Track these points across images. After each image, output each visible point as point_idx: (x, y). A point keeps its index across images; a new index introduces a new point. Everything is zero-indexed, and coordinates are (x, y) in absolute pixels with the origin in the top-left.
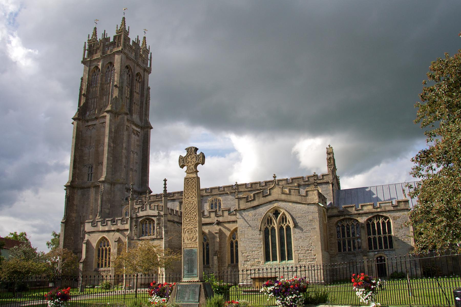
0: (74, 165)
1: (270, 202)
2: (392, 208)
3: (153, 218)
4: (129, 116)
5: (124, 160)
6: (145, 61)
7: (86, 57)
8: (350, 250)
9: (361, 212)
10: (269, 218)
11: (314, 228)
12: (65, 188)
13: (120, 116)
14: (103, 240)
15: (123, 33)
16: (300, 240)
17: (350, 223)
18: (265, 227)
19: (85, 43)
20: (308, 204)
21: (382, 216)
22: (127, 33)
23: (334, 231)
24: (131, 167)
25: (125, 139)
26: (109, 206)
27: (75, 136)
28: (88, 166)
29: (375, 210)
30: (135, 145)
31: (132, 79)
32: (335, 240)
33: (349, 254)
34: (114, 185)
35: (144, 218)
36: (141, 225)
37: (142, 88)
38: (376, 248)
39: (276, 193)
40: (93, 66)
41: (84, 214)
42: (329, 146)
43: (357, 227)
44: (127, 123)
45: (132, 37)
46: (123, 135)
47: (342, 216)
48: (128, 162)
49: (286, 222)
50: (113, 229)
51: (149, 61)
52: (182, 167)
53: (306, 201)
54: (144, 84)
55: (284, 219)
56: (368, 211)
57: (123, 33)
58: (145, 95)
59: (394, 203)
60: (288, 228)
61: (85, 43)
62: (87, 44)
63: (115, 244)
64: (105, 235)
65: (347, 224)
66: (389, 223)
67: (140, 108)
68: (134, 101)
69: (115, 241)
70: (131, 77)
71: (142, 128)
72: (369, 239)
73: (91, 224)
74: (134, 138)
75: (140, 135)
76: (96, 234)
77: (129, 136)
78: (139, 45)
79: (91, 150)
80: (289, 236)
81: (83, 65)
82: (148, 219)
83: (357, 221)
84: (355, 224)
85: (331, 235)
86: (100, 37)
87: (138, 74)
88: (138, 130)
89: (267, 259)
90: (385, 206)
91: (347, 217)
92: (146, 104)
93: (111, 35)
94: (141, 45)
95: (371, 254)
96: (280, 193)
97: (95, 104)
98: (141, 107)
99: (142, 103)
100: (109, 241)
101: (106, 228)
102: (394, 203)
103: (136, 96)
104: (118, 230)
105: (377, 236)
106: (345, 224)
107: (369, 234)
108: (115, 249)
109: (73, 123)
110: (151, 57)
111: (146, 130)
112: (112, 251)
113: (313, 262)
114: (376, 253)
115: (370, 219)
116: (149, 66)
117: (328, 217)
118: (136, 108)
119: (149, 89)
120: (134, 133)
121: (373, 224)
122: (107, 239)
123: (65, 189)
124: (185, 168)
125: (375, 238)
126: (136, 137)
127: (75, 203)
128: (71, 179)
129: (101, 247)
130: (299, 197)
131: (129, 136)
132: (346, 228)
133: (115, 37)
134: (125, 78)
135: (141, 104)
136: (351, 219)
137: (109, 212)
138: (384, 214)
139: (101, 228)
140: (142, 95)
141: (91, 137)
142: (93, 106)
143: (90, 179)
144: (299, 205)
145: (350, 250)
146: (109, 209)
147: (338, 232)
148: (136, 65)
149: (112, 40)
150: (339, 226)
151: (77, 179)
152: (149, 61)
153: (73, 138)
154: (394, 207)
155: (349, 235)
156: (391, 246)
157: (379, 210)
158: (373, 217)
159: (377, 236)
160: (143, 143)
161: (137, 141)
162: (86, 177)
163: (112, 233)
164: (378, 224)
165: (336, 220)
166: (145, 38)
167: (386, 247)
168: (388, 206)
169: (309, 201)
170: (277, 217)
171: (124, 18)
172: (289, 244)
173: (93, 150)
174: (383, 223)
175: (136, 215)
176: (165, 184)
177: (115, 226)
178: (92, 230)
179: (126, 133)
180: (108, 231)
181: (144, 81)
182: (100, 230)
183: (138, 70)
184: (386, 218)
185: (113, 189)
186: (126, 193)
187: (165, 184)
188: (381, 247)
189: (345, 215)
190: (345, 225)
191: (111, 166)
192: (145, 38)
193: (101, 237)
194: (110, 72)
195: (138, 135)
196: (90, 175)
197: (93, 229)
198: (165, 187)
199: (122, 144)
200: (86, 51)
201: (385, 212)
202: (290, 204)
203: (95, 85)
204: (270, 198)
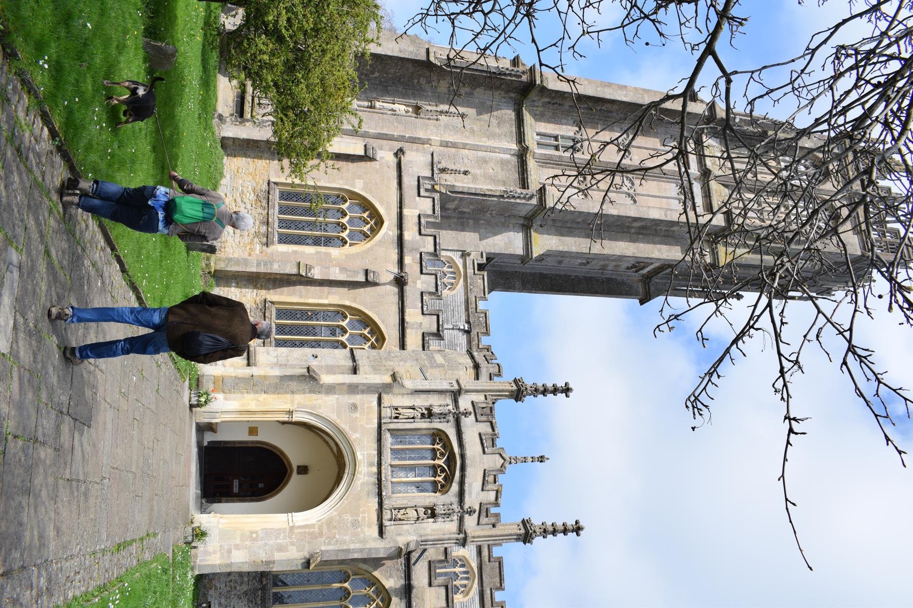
3: (455, 487)
28: (578, 136)
34: (523, 225)
35: (456, 450)
41: (443, 118)
50: (407, 260)
63: (356, 273)
64: (388, 229)
69: (367, 272)
73: (428, 174)
75: (631, 273)
82: (451, 460)
100: (369, 245)
101: (410, 234)
104: (400, 282)
108: (343, 269)
111: (640, 288)
112: (334, 252)
122: (375, 230)
127: (478, 90)
137: (449, 209)
139: (410, 214)
146: (455, 209)
151: (547, 100)
160: (609, 280)
163: (395, 257)
175: (466, 414)
178: (405, 179)
182: (406, 212)
185: (513, 221)
193: (382, 211)
195: (632, 267)
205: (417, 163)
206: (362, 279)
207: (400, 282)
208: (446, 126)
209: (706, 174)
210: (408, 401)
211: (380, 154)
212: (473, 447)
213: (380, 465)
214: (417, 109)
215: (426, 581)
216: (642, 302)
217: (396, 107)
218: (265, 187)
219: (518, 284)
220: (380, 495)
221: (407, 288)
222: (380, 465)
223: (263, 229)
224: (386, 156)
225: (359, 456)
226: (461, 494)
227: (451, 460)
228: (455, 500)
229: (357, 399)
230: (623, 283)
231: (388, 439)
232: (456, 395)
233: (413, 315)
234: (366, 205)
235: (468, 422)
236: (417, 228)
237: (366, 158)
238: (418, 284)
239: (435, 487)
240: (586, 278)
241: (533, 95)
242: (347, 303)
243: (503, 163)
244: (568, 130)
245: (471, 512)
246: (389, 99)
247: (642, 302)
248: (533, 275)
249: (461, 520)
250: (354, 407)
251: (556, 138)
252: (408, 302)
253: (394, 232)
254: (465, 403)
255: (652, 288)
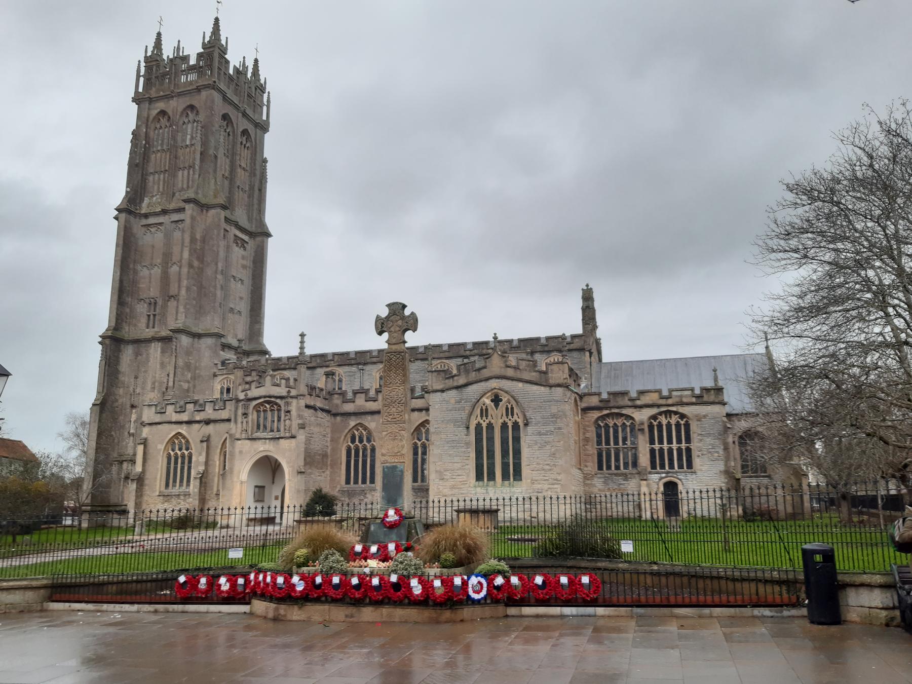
0: (120, 297)
1: (487, 379)
2: (694, 400)
3: (278, 401)
4: (228, 211)
5: (219, 293)
6: (257, 105)
7: (140, 90)
8: (617, 468)
9: (638, 403)
10: (484, 408)
11: (560, 428)
12: (100, 339)
13: (212, 212)
14: (178, 438)
15: (214, 49)
16: (536, 447)
17: (619, 422)
18: (476, 422)
19: (139, 62)
20: (551, 386)
21: (676, 413)
22: (223, 51)
23: (592, 434)
24: (232, 306)
25: (222, 254)
26: (189, 375)
27: (121, 243)
28: (147, 301)
29: (663, 402)
30: (240, 266)
31: (234, 142)
32: (592, 449)
33: (616, 475)
35: (262, 400)
36: (255, 413)
37: (251, 159)
38: (662, 466)
39: (496, 365)
40: (156, 109)
41: (138, 391)
42: (587, 285)
43: (631, 431)
44: (224, 225)
45: (234, 59)
46: (218, 246)
47: (606, 408)
48: (226, 297)
49: (512, 415)
50: (198, 418)
51: (265, 108)
52: (380, 333)
53: (547, 380)
54: (256, 151)
55: (509, 411)
56: (651, 402)
57: (214, 49)
58: (258, 173)
59: (697, 392)
60: (516, 426)
61: (139, 62)
62: (143, 64)
64: (183, 430)
65: (615, 424)
66: (687, 425)
67: (249, 197)
68: (238, 183)
69: (202, 441)
70: (231, 137)
71: (251, 234)
72: (652, 451)
73: (153, 408)
74: (237, 252)
75: (248, 247)
76: (166, 426)
77: (228, 247)
78: (246, 74)
79: (152, 272)
80: (517, 440)
81: (135, 107)
83: (632, 418)
84: (628, 424)
85: (587, 440)
86: (168, 52)
87: (245, 132)
88: (246, 238)
89: (479, 477)
90: (681, 396)
91: (616, 411)
92: (260, 190)
93: (193, 49)
94: (249, 75)
95: (655, 477)
96: (503, 365)
97: (161, 183)
98: (250, 196)
99: (252, 188)
100: (190, 440)
101: (184, 417)
102: (697, 392)
103: (242, 177)
104: (208, 422)
105: (665, 446)
106: (611, 422)
107: (652, 442)
108: (200, 454)
109: (116, 218)
110: (268, 101)
111: (259, 239)
112: (194, 459)
113: (556, 486)
114: (664, 475)
115: (654, 417)
116: (264, 118)
117: (582, 410)
118: (241, 197)
119: (265, 161)
120: (237, 243)
121: (660, 426)
122: (184, 437)
123: (100, 343)
124: (386, 336)
125: (661, 450)
126: (241, 252)
128: (113, 324)
129: (173, 450)
130: (534, 374)
131: (228, 247)
132: (611, 430)
133: (200, 55)
134: (222, 140)
135: (250, 189)
136: (622, 415)
137: (189, 388)
138: (681, 410)
139: (175, 417)
140: (253, 174)
141: (153, 247)
142: (156, 187)
143: (151, 325)
144: (535, 387)
145: (617, 468)
146: (189, 382)
147: (599, 436)
148: (240, 115)
149: (193, 62)
150: (599, 425)
152: (265, 108)
153: (117, 245)
154: (698, 397)
155: (616, 443)
156: (690, 465)
157: (670, 401)
158: (660, 414)
159: (665, 446)
160: (254, 262)
161: (243, 258)
162: (144, 321)
164: (669, 425)
165: (596, 414)
166: (256, 61)
167: (681, 466)
168: (686, 396)
169: (552, 382)
170: (497, 406)
171: (217, 20)
172: (517, 453)
173: (157, 271)
174: (678, 425)
176: (302, 342)
177: (202, 413)
178: (157, 420)
179: (222, 244)
180: (189, 423)
181: (256, 147)
182: (173, 420)
183: (242, 124)
184: (682, 416)
186: (222, 353)
187: (302, 342)
188: (671, 466)
189: (611, 408)
190: (611, 425)
191: (194, 302)
192: (256, 61)
193: (173, 433)
194: (190, 126)
196: (152, 317)
197: (158, 418)
198: (302, 348)
199: (216, 264)
200: (142, 79)
201: (682, 404)
202: (520, 385)
203: (159, 148)
204: (486, 373)
205: (149, 415)
206: (205, 444)
207: (208, 422)
208: (143, 388)
209: (164, 212)
210: (239, 425)
211: (144, 435)
212: (261, 392)
213: (265, 439)
214: (133, 406)
215: (352, 404)
216: (269, 235)
217: (133, 420)
218: (161, 498)
219: (257, 326)
220: (278, 438)
221: (213, 417)
222: (265, 439)
223: (182, 497)
224: (146, 432)
225: (262, 449)
226: (281, 398)
227: (268, 402)
228: (284, 401)
229: (237, 451)
230: (256, 252)
231: (259, 434)
232: (238, 401)
233: (224, 415)
234: (171, 442)
235: (251, 394)
236: (182, 414)
237: (145, 442)
238: (209, 413)
239: (279, 410)
240: (253, 279)
241: (119, 335)
242: (219, 450)
243: (163, 352)
244: (142, 309)
245: (289, 392)
246: (127, 426)
247: (269, 235)
248: (251, 316)
249: (292, 397)
250: (241, 452)
251: (149, 316)
252: (219, 418)
253: (184, 426)
254: (241, 396)
255: (259, 230)
